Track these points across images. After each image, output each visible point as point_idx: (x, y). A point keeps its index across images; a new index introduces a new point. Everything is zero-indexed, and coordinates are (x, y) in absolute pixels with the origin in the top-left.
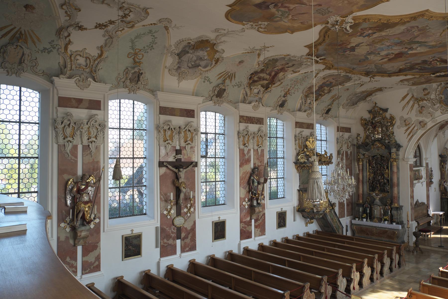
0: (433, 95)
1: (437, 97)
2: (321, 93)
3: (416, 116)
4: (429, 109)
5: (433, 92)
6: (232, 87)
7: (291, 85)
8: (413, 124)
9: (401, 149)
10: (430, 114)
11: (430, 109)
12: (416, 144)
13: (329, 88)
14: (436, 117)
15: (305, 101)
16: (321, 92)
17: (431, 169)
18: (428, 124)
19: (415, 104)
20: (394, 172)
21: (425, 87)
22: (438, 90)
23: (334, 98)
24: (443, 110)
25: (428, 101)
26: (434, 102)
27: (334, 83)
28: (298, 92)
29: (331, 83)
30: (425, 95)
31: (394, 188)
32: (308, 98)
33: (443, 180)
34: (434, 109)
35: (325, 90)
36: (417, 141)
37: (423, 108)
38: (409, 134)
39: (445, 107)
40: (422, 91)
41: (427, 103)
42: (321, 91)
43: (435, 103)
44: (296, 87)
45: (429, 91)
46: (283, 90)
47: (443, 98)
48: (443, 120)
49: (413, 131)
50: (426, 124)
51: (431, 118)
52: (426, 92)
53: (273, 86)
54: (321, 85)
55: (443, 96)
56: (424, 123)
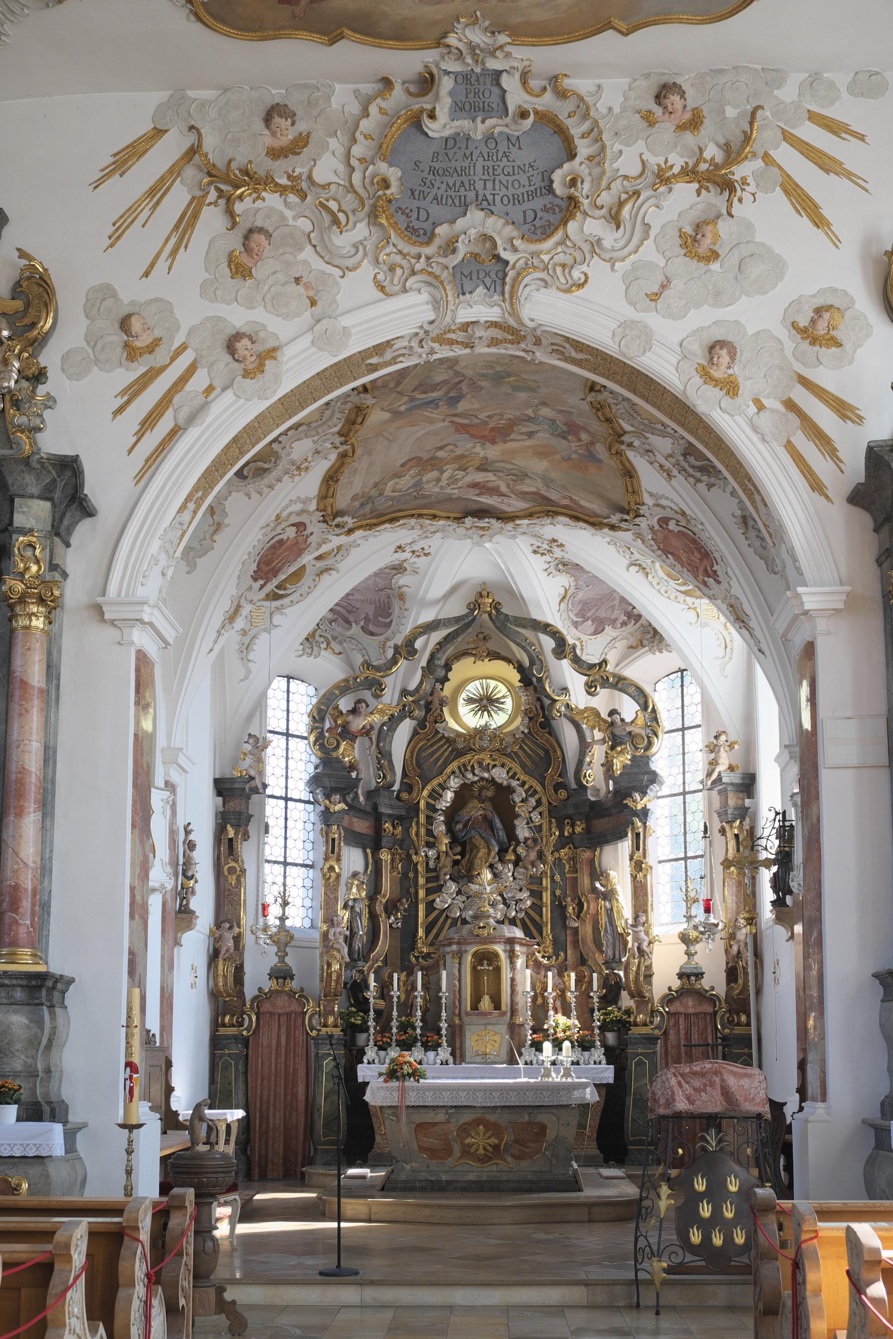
0: (327, 156)
1: (357, 178)
3: (208, 290)
4: (301, 249)
5: (333, 143)
8: (183, 348)
9: (83, 532)
10: (300, 289)
11: (307, 253)
12: (191, 506)
14: (343, 314)
17: (187, 832)
18: (288, 353)
19: (205, 208)
20: (24, 684)
21: (277, 100)
22: (365, 125)
24: (392, 269)
25: (293, 198)
26: (333, 205)
30: (275, 154)
31: (20, 814)
33: (231, 928)
34: (328, 254)
36: (196, 489)
37: (261, 238)
38: (149, 422)
39: (407, 248)
40: (259, 126)
41: (289, 214)
43: (341, 216)
45: (302, 126)
47: (393, 190)
48: (379, 349)
49: (177, 399)
50: (272, 353)
51: (307, 316)
52: (288, 133)
55: (393, 174)
56: (259, 348)
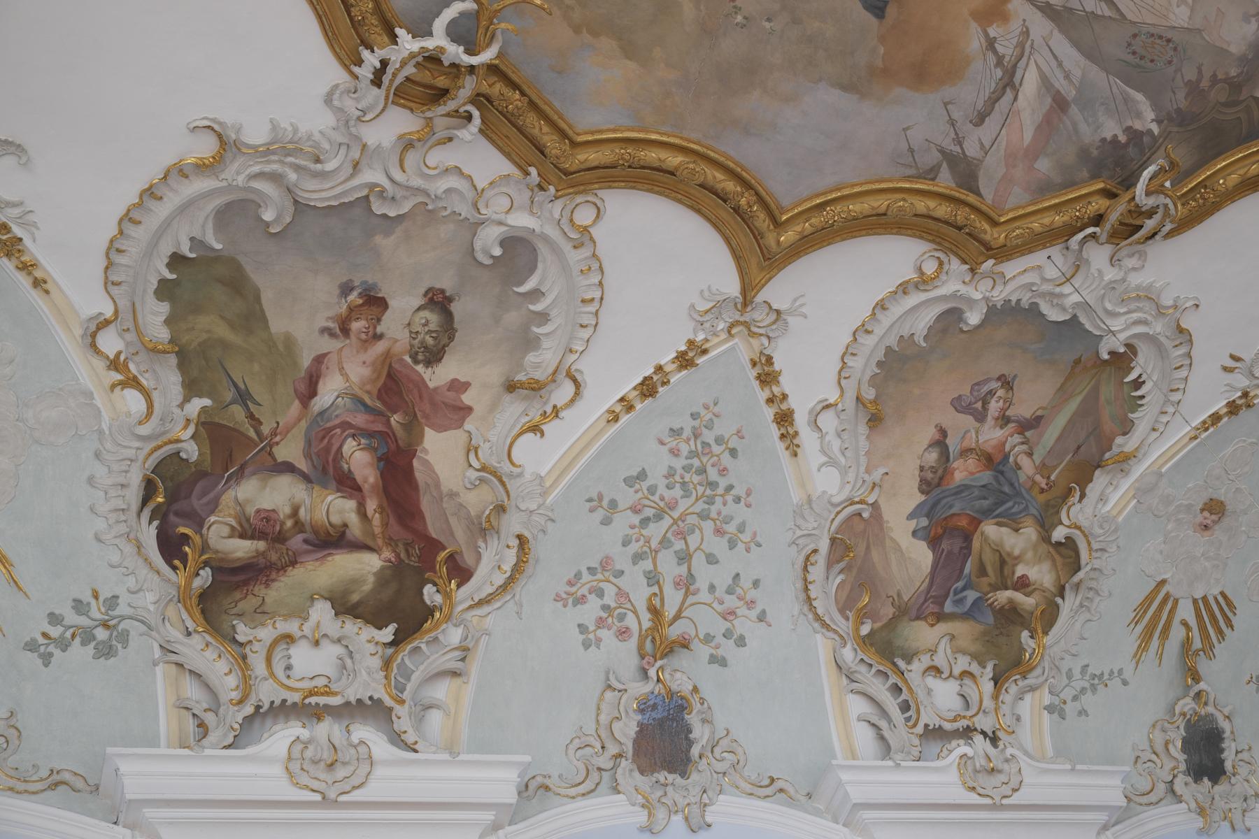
2: (1011, 601)
6: (32, 659)
7: (637, 558)
13: (1030, 532)
15: (896, 689)
16: (995, 588)
23: (1177, 633)
27: (1025, 462)
28: (762, 618)
29: (995, 461)
32: (909, 658)
35: (1018, 559)
42: (982, 571)
44: (704, 574)
46: (600, 623)
53: (464, 595)
54: (926, 510)
